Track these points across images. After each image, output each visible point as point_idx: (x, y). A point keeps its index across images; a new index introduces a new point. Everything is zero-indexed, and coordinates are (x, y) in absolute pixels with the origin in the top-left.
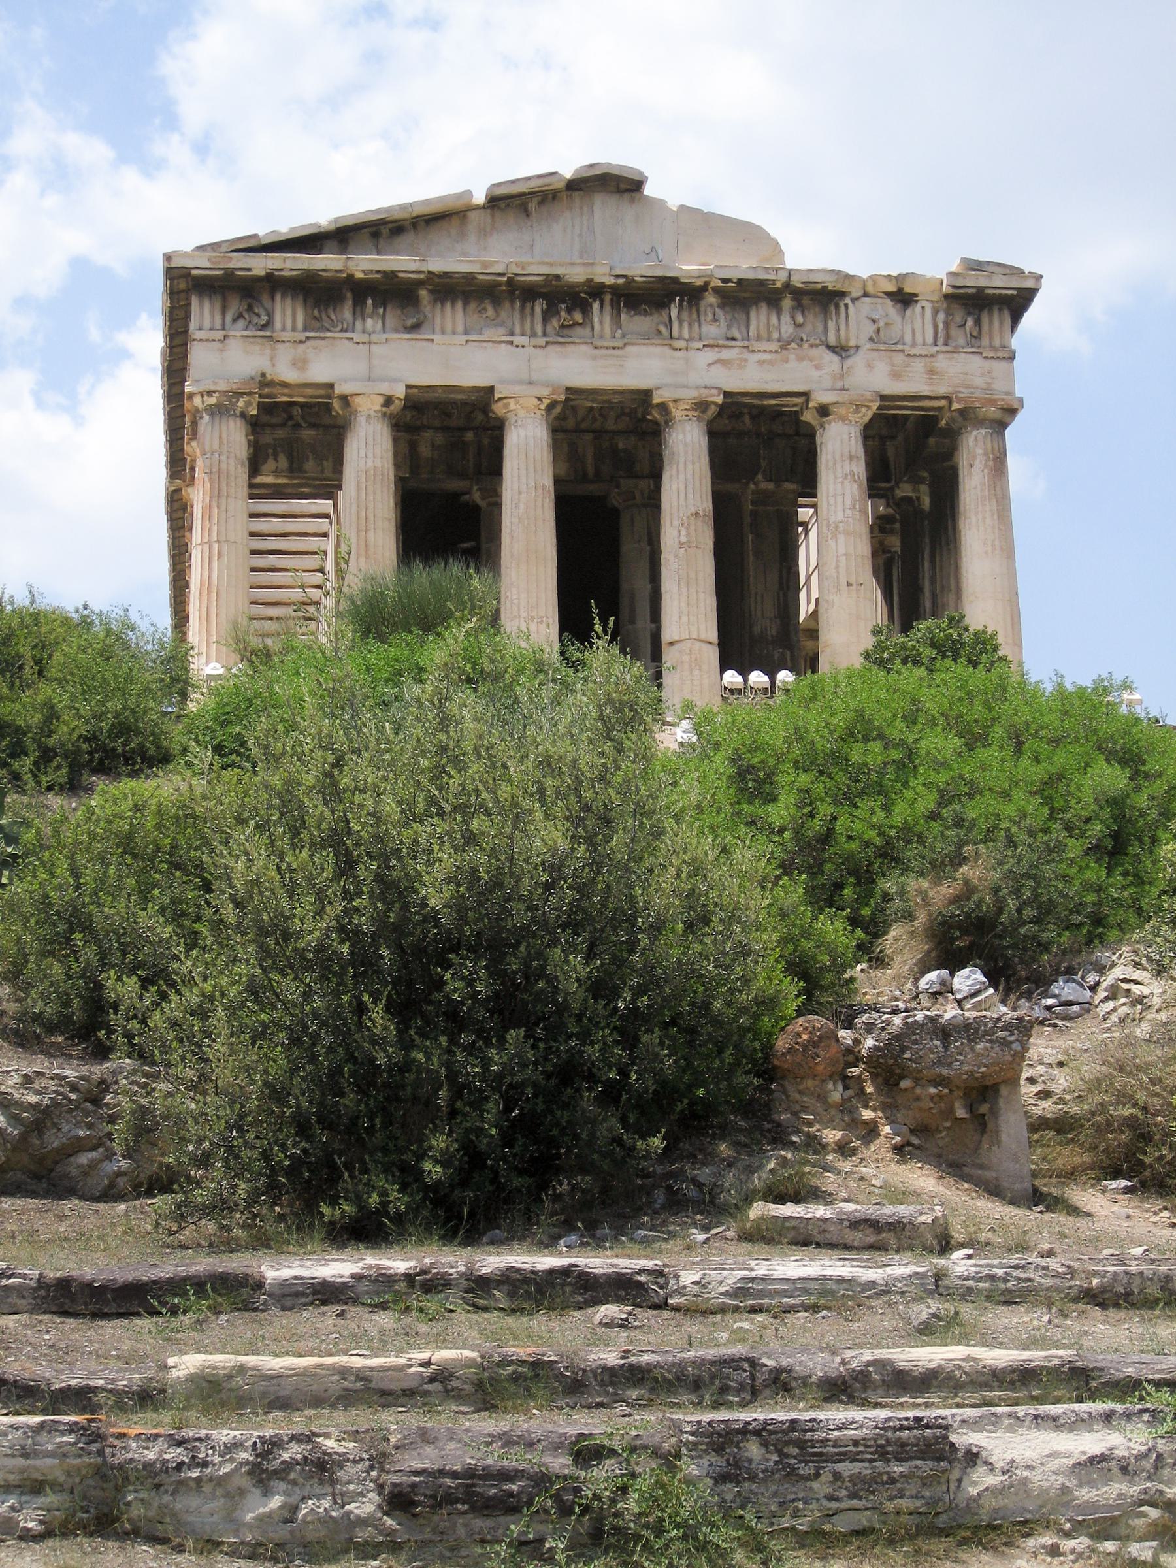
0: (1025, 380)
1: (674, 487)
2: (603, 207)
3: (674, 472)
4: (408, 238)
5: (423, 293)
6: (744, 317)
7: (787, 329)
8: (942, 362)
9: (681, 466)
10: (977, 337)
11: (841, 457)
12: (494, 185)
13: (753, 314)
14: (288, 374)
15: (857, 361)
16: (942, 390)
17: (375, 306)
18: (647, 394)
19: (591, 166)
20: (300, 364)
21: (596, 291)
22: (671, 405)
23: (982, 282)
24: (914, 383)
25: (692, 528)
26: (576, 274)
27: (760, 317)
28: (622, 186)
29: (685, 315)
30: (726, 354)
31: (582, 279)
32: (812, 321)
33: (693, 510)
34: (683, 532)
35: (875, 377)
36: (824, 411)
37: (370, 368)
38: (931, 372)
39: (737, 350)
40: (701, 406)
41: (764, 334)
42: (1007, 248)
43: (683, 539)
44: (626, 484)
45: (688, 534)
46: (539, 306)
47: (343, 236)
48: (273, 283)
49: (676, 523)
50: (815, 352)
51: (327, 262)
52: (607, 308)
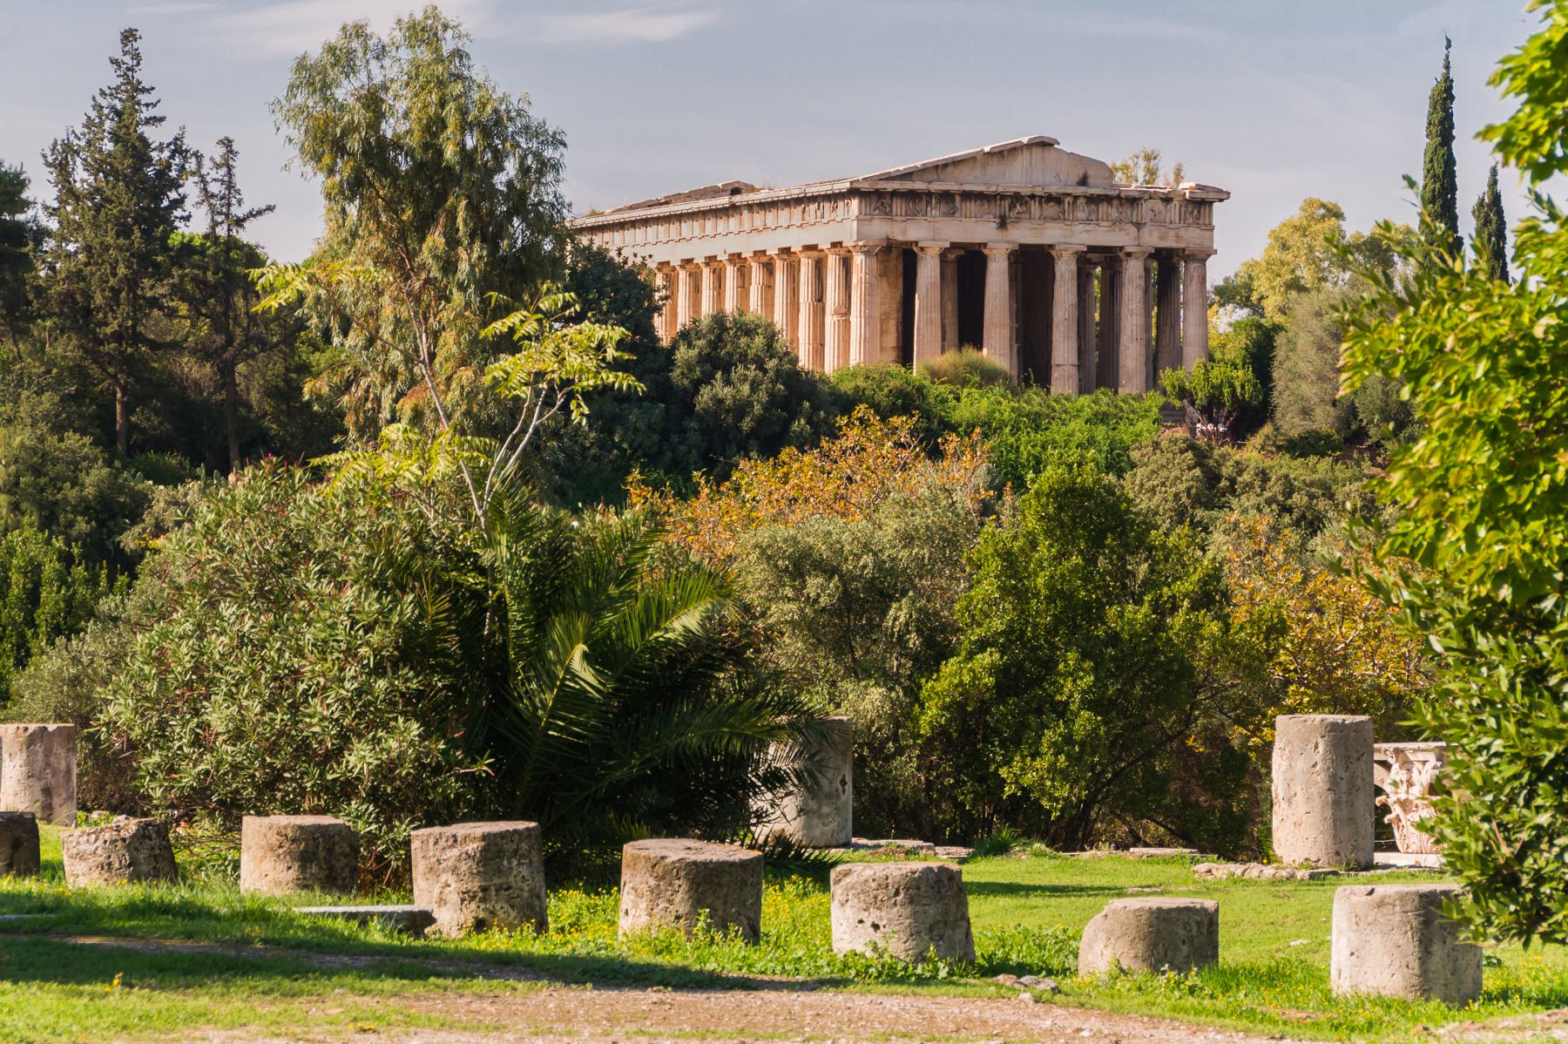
0: (1219, 240)
2: (1037, 153)
4: (950, 168)
5: (958, 198)
7: (1114, 212)
8: (1182, 232)
10: (1198, 218)
11: (1133, 272)
14: (900, 238)
15: (1145, 231)
16: (1182, 245)
18: (1051, 246)
20: (904, 232)
21: (1033, 197)
23: (1204, 196)
24: (1170, 243)
26: (1025, 191)
27: (1103, 207)
28: (1045, 144)
32: (1127, 210)
35: (1153, 239)
36: (1129, 255)
37: (932, 233)
38: (1178, 236)
42: (1214, 179)
46: (1007, 203)
47: (923, 171)
48: (895, 194)
51: (919, 185)
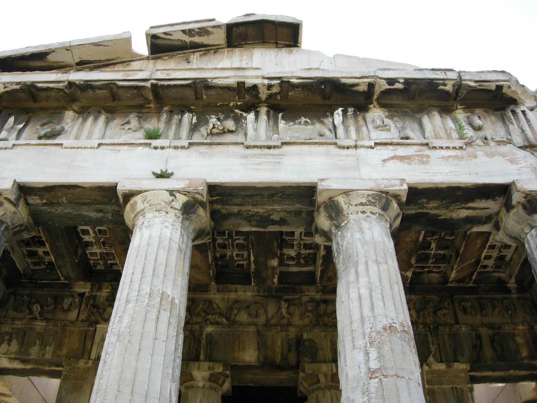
1: (354, 295)
3: (352, 277)
6: (416, 126)
9: (361, 268)
12: (152, 28)
13: (425, 120)
17: (16, 122)
19: (248, 15)
22: (341, 200)
25: (386, 348)
27: (434, 123)
29: (351, 122)
30: (402, 151)
31: (232, 81)
33: (385, 322)
34: (373, 355)
39: (415, 148)
40: (382, 199)
41: (442, 134)
43: (374, 365)
44: (309, 368)
45: (380, 357)
49: (360, 342)
50: (503, 149)
52: (263, 117)
